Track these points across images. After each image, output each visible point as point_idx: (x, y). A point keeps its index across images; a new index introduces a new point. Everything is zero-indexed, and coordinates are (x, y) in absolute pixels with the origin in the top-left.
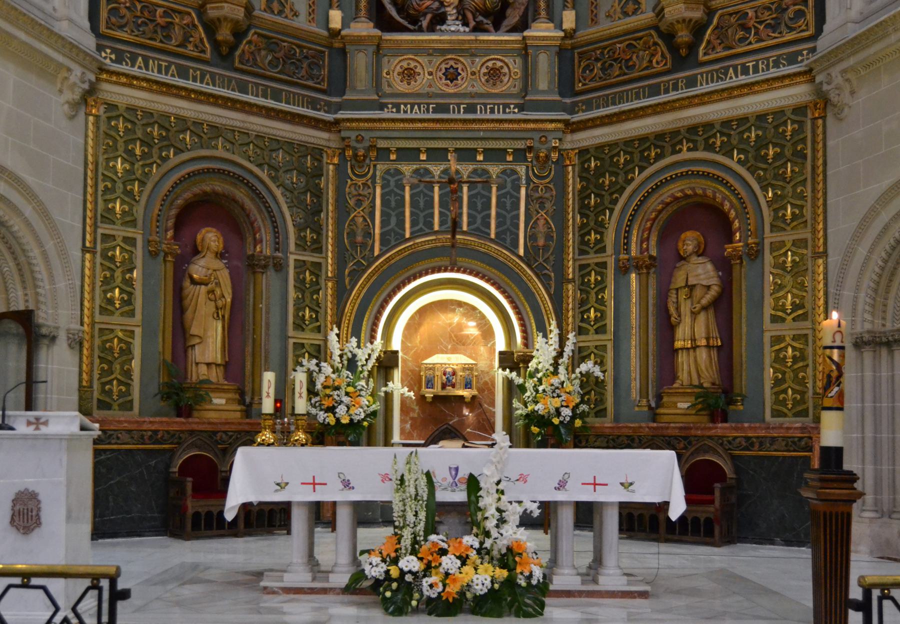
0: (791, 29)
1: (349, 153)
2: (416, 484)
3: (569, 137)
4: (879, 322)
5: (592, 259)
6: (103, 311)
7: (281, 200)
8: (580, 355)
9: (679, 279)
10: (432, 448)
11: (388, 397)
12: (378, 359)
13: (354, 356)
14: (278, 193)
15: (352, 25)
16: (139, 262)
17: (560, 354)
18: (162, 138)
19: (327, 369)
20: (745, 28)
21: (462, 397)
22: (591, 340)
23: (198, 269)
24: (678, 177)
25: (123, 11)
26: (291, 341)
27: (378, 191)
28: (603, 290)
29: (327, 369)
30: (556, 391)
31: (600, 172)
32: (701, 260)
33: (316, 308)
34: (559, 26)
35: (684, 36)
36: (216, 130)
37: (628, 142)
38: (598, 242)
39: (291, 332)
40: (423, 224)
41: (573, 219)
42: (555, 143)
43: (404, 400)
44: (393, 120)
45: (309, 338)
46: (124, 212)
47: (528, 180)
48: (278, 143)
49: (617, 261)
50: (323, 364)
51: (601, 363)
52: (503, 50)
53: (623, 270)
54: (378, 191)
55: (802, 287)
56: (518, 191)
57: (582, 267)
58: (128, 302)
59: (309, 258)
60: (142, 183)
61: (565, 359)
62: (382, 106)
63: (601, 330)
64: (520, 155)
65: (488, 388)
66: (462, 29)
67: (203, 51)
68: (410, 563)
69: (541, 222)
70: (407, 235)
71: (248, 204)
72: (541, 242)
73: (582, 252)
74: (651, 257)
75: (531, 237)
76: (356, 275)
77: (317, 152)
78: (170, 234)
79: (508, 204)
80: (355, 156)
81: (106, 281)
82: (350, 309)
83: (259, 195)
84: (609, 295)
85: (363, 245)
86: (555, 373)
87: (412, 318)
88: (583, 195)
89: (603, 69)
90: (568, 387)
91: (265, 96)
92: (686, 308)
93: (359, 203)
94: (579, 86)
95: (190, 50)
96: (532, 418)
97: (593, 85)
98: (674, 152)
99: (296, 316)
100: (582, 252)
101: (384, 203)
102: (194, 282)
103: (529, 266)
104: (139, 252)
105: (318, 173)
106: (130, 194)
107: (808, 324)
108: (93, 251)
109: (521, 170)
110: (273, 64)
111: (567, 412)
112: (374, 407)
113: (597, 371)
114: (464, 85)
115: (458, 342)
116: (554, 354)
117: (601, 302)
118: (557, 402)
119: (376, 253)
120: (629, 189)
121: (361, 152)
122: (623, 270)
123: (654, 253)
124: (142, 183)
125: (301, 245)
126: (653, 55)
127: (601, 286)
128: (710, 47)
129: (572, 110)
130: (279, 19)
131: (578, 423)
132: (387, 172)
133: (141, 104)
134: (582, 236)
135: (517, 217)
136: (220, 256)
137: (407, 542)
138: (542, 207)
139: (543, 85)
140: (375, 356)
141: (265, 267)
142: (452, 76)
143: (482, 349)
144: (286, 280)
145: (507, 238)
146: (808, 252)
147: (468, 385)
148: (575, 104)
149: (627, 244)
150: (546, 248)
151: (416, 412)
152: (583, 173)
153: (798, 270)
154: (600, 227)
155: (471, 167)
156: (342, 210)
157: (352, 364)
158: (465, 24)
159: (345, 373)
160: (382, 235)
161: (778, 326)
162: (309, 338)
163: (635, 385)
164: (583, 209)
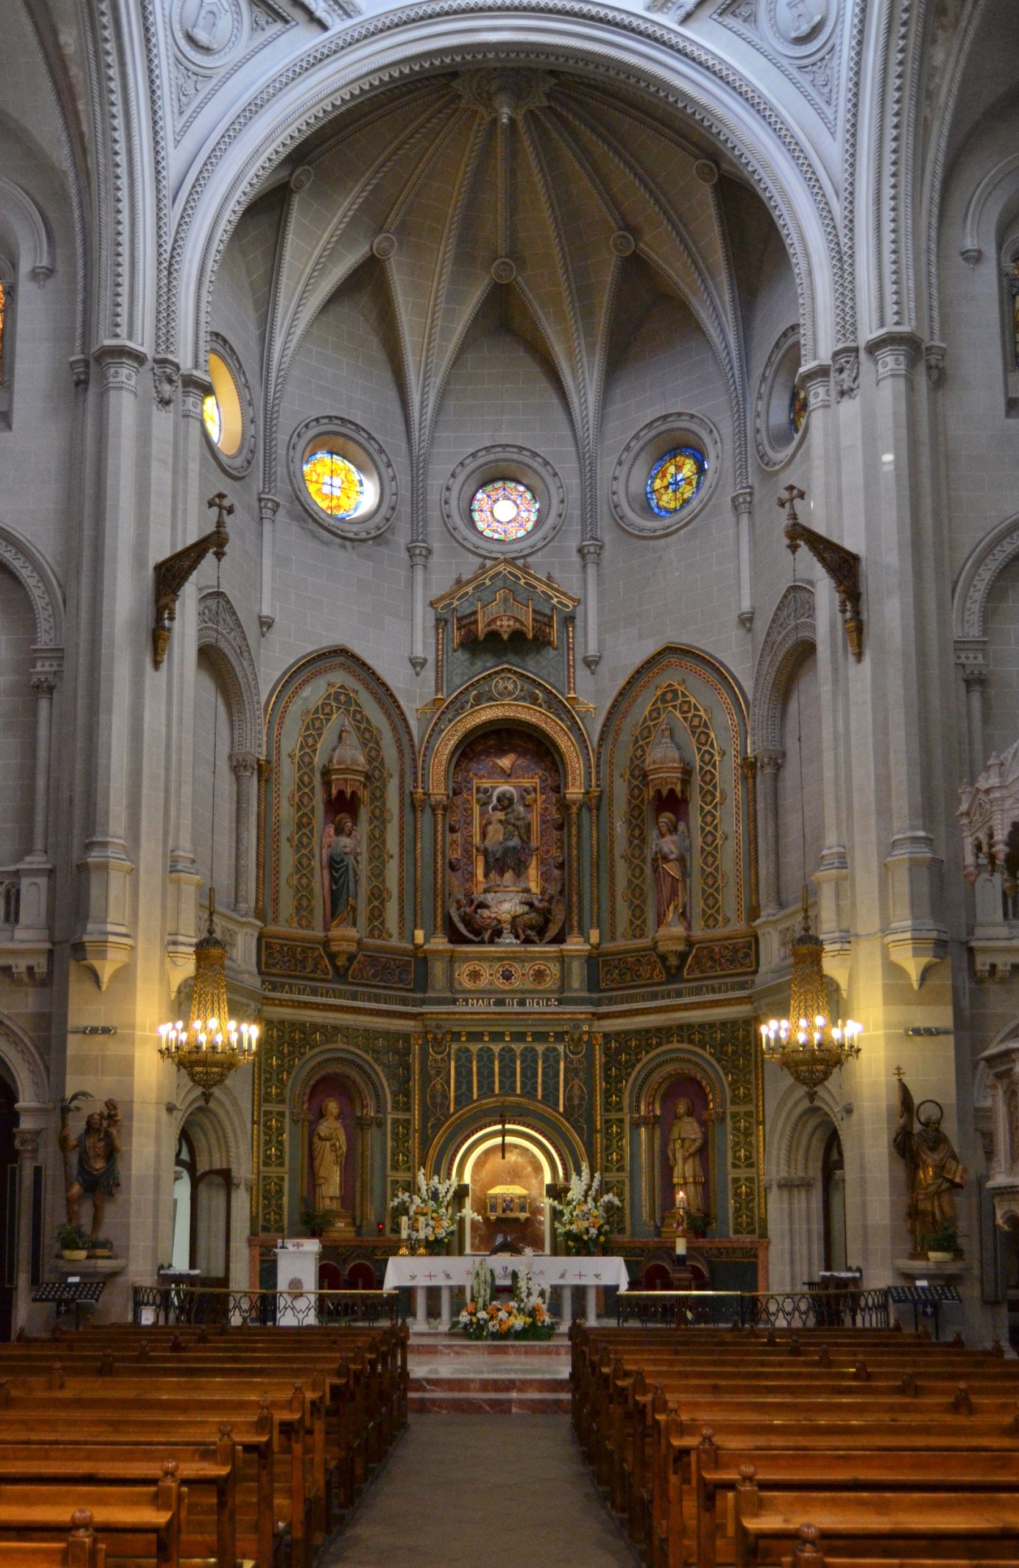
0: (742, 965)
1: (430, 1036)
2: (485, 1275)
3: (596, 1023)
4: (793, 1171)
5: (614, 1115)
6: (266, 1164)
7: (381, 1075)
8: (605, 1188)
9: (675, 1134)
10: (494, 1257)
11: (462, 1221)
12: (455, 1193)
13: (437, 1189)
14: (378, 1069)
15: (433, 940)
16: (287, 1130)
17: (589, 1187)
18: (300, 1039)
19: (417, 1200)
20: (712, 959)
21: (517, 1220)
22: (612, 1176)
23: (324, 1128)
24: (673, 1060)
25: (276, 955)
26: (389, 1179)
27: (453, 1064)
28: (621, 1139)
29: (417, 1200)
30: (586, 1216)
31: (618, 1052)
32: (690, 1119)
33: (407, 1152)
34: (587, 941)
35: (673, 961)
36: (335, 1028)
37: (638, 1032)
38: (618, 1103)
39: (389, 1172)
40: (486, 1088)
41: (600, 1084)
42: (585, 1028)
43: (474, 1223)
44: (463, 1013)
45: (402, 1176)
46: (277, 1094)
47: (566, 1055)
48: (378, 1034)
49: (631, 1118)
50: (415, 1197)
51: (620, 1195)
52: (546, 958)
53: (636, 1125)
54: (453, 1064)
55: (750, 1144)
56: (558, 1064)
57: (607, 1121)
58: (280, 1157)
59: (402, 1116)
60: (289, 1073)
61: (592, 1193)
62: (454, 1002)
63: (620, 1169)
64: (559, 1036)
65: (537, 1211)
66: (515, 941)
67: (327, 974)
68: (482, 1315)
69: (576, 1087)
70: (475, 1097)
71: (359, 1080)
72: (576, 1102)
73: (607, 1110)
74: (655, 1116)
75: (568, 1099)
76: (437, 1127)
77: (406, 1037)
78: (306, 1106)
79: (551, 1074)
80: (435, 1039)
81: (267, 1143)
82: (433, 1153)
83: (365, 1072)
84: (626, 1142)
85: (442, 1105)
86: (586, 1202)
87: (479, 1158)
88: (606, 1068)
89: (620, 975)
90: (595, 1212)
91: (370, 1001)
92: (679, 1155)
93: (438, 1073)
94: (603, 986)
95: (319, 975)
96: (569, 1235)
97: (613, 985)
98: (669, 1042)
99: (392, 1159)
100: (607, 1110)
101: (458, 1073)
102: (321, 1138)
103: (568, 1120)
104: (287, 1120)
105: (408, 1052)
106: (281, 1081)
107: (754, 1170)
108: (258, 1124)
109: (561, 1048)
110: (374, 976)
111: (593, 1231)
112: (452, 1228)
113: (616, 1201)
114: (516, 984)
115: (514, 1176)
116: (585, 1187)
117: (621, 1148)
118: (586, 1224)
119: (452, 1110)
120: (638, 1067)
121: (439, 1036)
122: (636, 1125)
123: (658, 1113)
124: (289, 1073)
125: (396, 1107)
126: (653, 970)
127: (620, 1135)
128: (691, 970)
129: (598, 1003)
130: (379, 942)
131: (602, 1239)
132: (459, 1050)
133: (288, 1017)
134: (607, 1098)
135: (558, 1083)
136: (340, 1116)
137: (481, 1304)
138: (576, 1075)
139: (576, 984)
140: (452, 1190)
141: (370, 1125)
142: (507, 976)
143: (534, 1181)
144: (385, 1135)
145: (550, 1097)
146: (753, 1120)
147: (523, 1209)
148: (600, 999)
149: (638, 1102)
150: (580, 1106)
151: (483, 1231)
152: (606, 1050)
153: (748, 1133)
154: (619, 1092)
155: (522, 1046)
156: (426, 1079)
157: (435, 1195)
158: (517, 937)
159: (431, 1203)
160: (456, 1098)
161: (737, 1171)
162: (402, 1176)
163: (645, 1211)
164: (607, 1078)
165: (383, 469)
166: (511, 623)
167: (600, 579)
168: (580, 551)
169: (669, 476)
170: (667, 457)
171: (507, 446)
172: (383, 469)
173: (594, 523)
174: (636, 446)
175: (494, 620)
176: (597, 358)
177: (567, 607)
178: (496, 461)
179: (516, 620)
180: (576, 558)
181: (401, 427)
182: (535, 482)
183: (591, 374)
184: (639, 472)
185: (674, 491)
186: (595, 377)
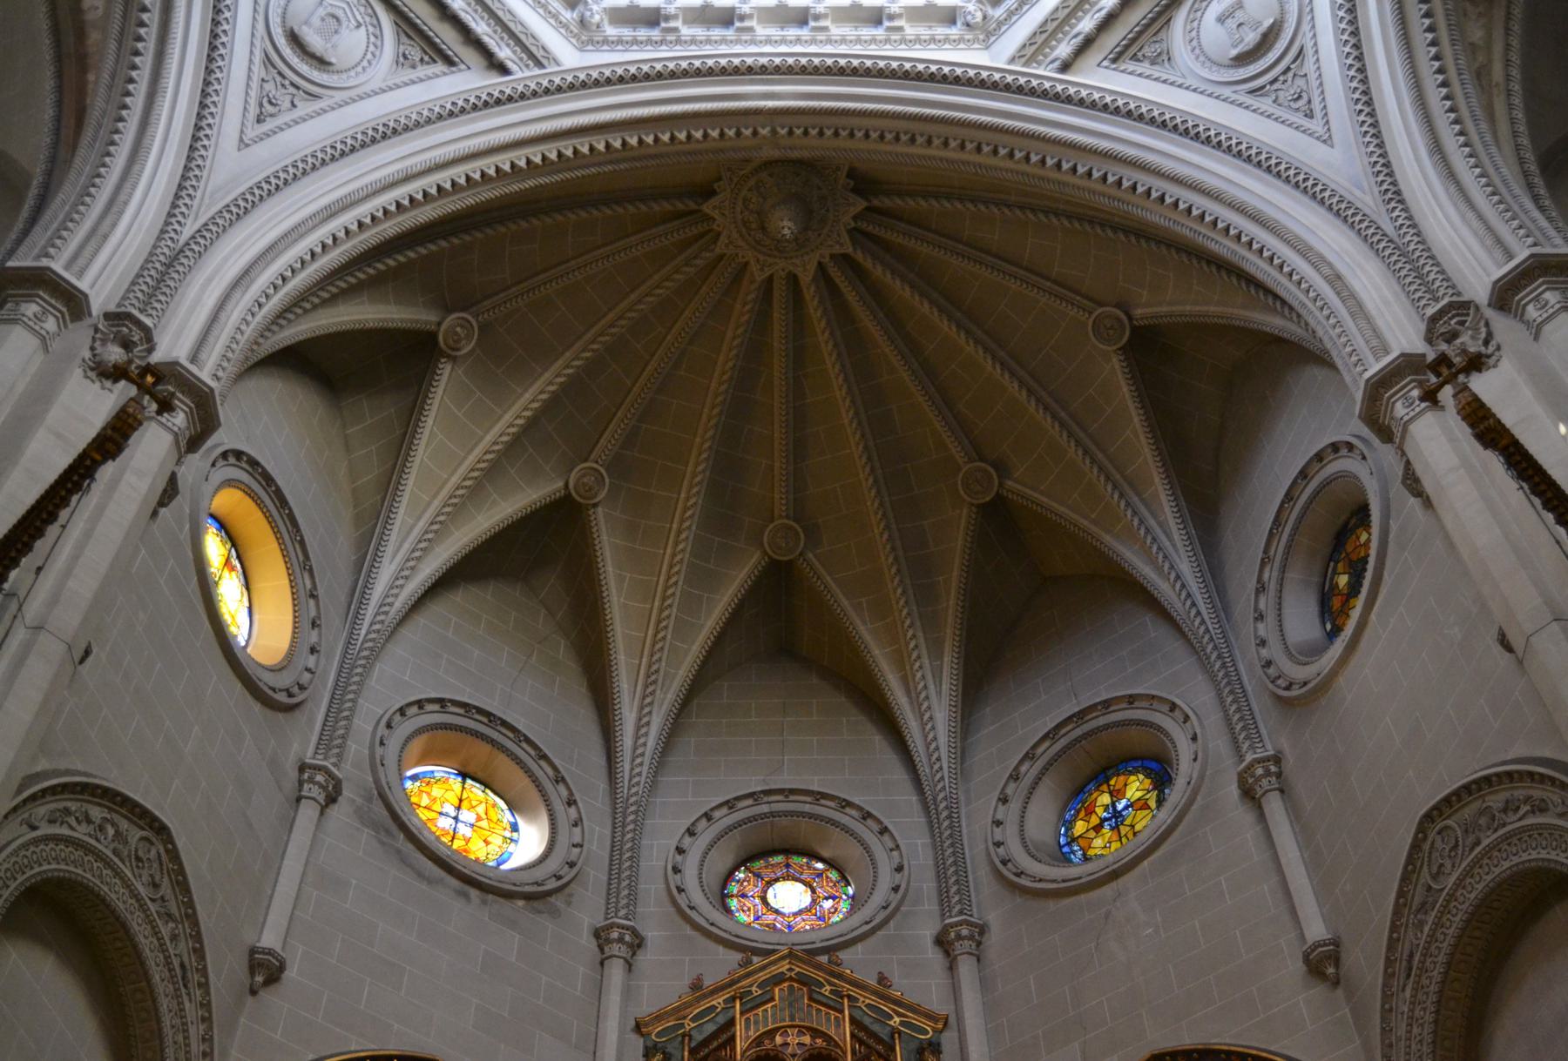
165: (559, 807)
166: (807, 1039)
167: (985, 984)
168: (942, 942)
169: (1099, 811)
170: (1092, 786)
171: (793, 791)
172: (559, 807)
173: (963, 890)
174: (1030, 771)
175: (771, 1034)
176: (947, 659)
177: (926, 1032)
178: (773, 814)
179: (815, 1033)
180: (934, 956)
181: (601, 761)
182: (850, 852)
183: (939, 684)
184: (1041, 817)
185: (1115, 828)
186: (945, 687)
